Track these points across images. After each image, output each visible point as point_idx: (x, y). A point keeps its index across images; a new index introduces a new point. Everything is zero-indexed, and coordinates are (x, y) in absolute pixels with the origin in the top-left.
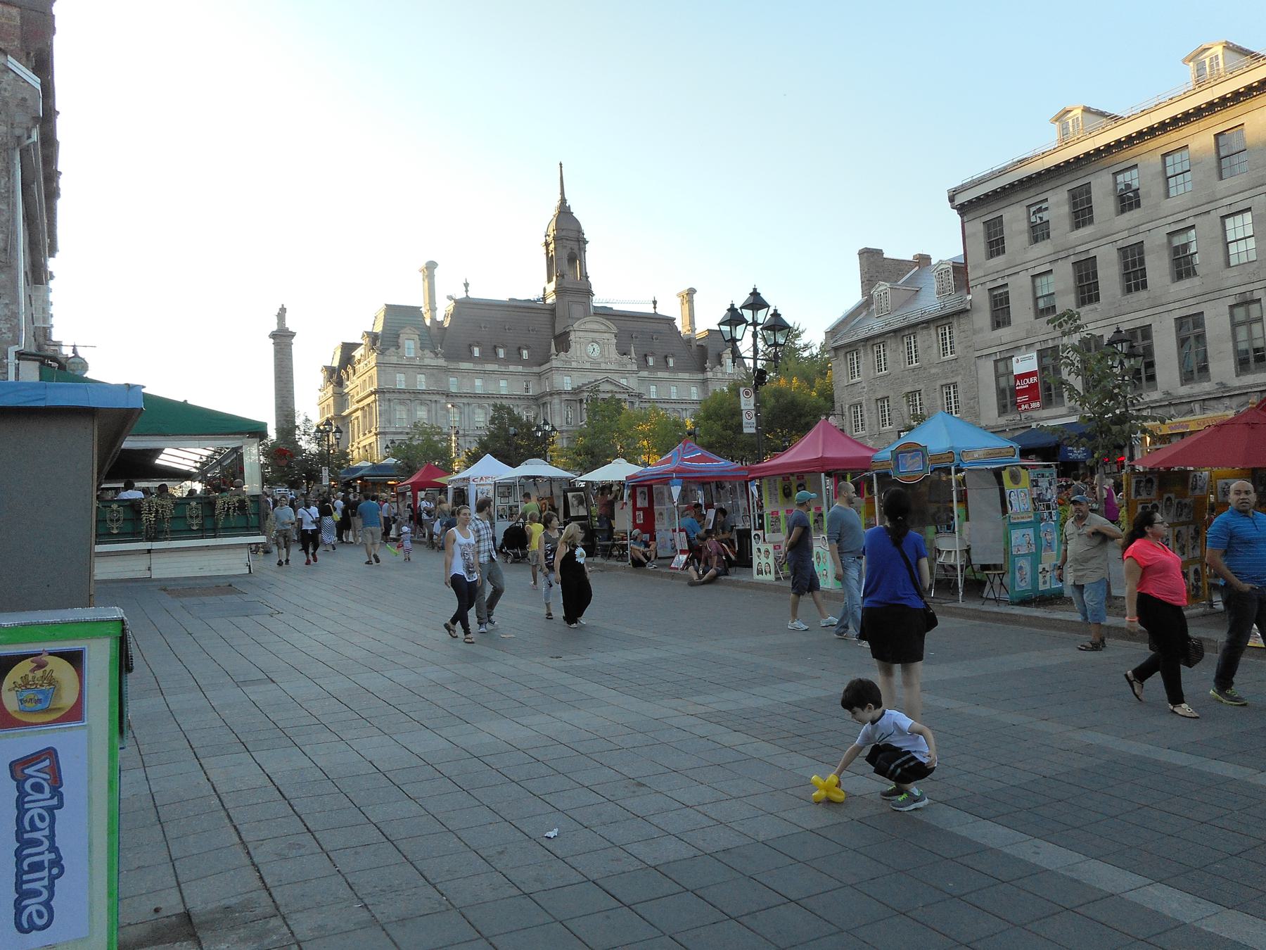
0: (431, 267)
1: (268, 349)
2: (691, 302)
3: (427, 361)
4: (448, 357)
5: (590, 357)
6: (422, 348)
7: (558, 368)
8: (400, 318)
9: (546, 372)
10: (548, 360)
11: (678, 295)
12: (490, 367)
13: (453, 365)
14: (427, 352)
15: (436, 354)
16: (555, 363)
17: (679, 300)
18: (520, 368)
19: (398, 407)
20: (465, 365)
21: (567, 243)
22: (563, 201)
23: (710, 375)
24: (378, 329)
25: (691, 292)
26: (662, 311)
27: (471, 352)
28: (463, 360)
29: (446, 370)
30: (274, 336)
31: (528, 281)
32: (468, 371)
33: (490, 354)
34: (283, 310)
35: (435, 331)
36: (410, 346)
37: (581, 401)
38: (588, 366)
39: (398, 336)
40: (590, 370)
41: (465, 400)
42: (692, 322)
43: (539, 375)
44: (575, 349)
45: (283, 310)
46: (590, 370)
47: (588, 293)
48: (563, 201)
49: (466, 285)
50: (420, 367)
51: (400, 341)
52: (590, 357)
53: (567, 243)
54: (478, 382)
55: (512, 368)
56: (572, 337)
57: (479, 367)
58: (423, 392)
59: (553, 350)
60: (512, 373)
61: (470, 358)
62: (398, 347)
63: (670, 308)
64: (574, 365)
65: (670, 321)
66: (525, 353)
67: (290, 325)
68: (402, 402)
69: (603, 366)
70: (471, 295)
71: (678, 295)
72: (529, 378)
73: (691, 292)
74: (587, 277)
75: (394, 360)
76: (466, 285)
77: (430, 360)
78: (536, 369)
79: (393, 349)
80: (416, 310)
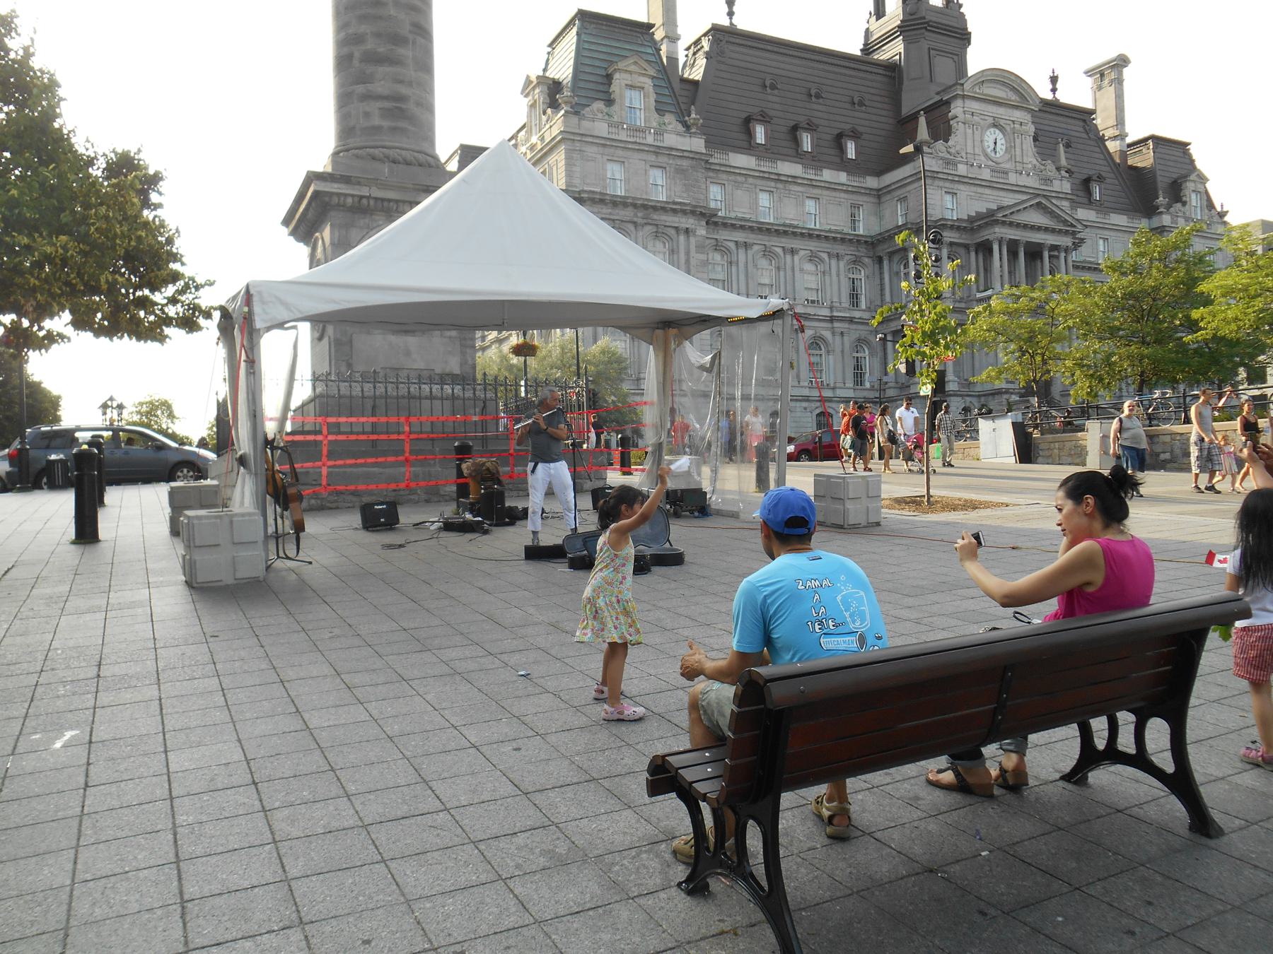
2: (1119, 82)
3: (671, 140)
5: (983, 162)
6: (660, 111)
7: (934, 176)
9: (902, 184)
11: (1089, 73)
12: (788, 168)
14: (669, 118)
15: (687, 127)
16: (931, 164)
17: (1089, 81)
18: (842, 177)
20: (741, 160)
23: (1166, 220)
24: (563, 69)
25: (1121, 62)
26: (1068, 96)
27: (750, 134)
32: (745, 174)
33: (787, 142)
36: (636, 99)
37: (985, 249)
38: (986, 174)
39: (609, 78)
40: (990, 185)
41: (740, 236)
42: (1120, 122)
43: (879, 195)
44: (960, 138)
46: (990, 185)
47: (964, 37)
50: (657, 151)
51: (613, 88)
52: (983, 162)
54: (764, 200)
55: (828, 175)
56: (957, 109)
57: (766, 167)
58: (662, 208)
59: (923, 133)
60: (831, 187)
61: (749, 146)
62: (610, 102)
63: (1077, 92)
64: (962, 170)
65: (1084, 116)
66: (851, 150)
69: (1013, 178)
71: (1089, 73)
72: (860, 199)
73: (1121, 62)
75: (601, 128)
77: (675, 139)
78: (872, 182)
79: (599, 105)
80: (645, 29)
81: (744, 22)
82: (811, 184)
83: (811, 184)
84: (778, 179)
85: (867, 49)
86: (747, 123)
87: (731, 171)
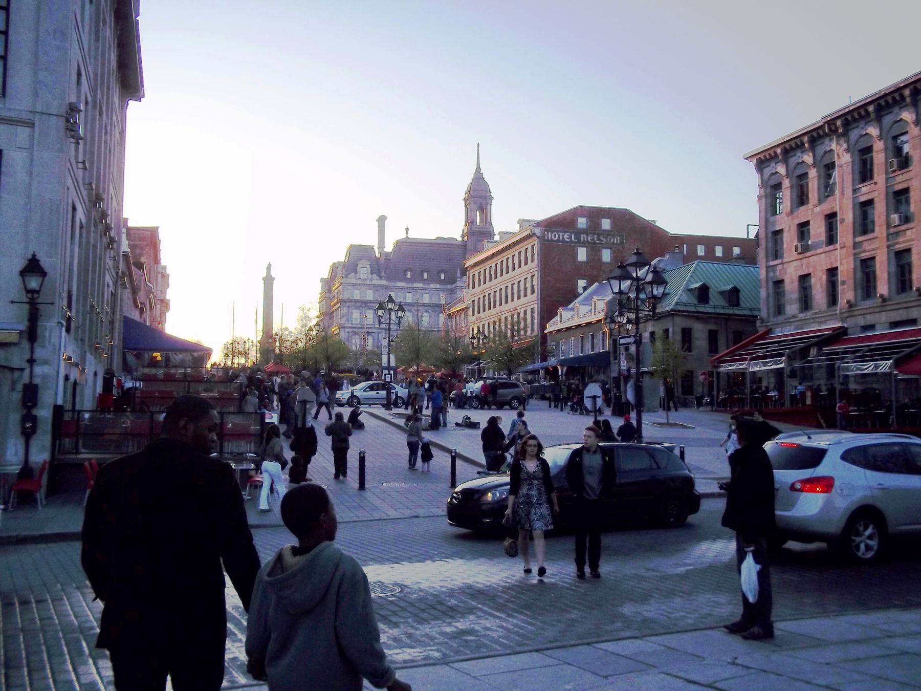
0: (382, 220)
1: (261, 285)
3: (374, 282)
4: (388, 279)
6: (372, 273)
8: (358, 254)
10: (454, 282)
13: (391, 284)
14: (375, 276)
15: (381, 277)
16: (459, 284)
18: (438, 286)
19: (354, 311)
21: (479, 197)
22: (478, 169)
28: (401, 281)
29: (387, 288)
30: (263, 279)
31: (450, 225)
32: (402, 288)
34: (269, 266)
35: (382, 260)
36: (364, 271)
45: (269, 266)
48: (478, 169)
49: (407, 229)
53: (479, 197)
55: (432, 286)
58: (370, 302)
59: (459, 275)
61: (405, 279)
67: (273, 274)
68: (357, 308)
70: (410, 236)
74: (491, 223)
75: (353, 281)
76: (407, 229)
77: (376, 281)
78: (449, 287)
79: (353, 274)
81: (413, 235)
82: (426, 289)
83: (426, 289)
84: (413, 288)
85: (463, 236)
86: (405, 272)
87: (395, 287)
